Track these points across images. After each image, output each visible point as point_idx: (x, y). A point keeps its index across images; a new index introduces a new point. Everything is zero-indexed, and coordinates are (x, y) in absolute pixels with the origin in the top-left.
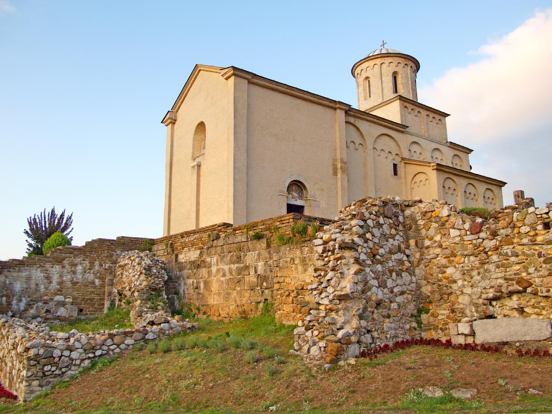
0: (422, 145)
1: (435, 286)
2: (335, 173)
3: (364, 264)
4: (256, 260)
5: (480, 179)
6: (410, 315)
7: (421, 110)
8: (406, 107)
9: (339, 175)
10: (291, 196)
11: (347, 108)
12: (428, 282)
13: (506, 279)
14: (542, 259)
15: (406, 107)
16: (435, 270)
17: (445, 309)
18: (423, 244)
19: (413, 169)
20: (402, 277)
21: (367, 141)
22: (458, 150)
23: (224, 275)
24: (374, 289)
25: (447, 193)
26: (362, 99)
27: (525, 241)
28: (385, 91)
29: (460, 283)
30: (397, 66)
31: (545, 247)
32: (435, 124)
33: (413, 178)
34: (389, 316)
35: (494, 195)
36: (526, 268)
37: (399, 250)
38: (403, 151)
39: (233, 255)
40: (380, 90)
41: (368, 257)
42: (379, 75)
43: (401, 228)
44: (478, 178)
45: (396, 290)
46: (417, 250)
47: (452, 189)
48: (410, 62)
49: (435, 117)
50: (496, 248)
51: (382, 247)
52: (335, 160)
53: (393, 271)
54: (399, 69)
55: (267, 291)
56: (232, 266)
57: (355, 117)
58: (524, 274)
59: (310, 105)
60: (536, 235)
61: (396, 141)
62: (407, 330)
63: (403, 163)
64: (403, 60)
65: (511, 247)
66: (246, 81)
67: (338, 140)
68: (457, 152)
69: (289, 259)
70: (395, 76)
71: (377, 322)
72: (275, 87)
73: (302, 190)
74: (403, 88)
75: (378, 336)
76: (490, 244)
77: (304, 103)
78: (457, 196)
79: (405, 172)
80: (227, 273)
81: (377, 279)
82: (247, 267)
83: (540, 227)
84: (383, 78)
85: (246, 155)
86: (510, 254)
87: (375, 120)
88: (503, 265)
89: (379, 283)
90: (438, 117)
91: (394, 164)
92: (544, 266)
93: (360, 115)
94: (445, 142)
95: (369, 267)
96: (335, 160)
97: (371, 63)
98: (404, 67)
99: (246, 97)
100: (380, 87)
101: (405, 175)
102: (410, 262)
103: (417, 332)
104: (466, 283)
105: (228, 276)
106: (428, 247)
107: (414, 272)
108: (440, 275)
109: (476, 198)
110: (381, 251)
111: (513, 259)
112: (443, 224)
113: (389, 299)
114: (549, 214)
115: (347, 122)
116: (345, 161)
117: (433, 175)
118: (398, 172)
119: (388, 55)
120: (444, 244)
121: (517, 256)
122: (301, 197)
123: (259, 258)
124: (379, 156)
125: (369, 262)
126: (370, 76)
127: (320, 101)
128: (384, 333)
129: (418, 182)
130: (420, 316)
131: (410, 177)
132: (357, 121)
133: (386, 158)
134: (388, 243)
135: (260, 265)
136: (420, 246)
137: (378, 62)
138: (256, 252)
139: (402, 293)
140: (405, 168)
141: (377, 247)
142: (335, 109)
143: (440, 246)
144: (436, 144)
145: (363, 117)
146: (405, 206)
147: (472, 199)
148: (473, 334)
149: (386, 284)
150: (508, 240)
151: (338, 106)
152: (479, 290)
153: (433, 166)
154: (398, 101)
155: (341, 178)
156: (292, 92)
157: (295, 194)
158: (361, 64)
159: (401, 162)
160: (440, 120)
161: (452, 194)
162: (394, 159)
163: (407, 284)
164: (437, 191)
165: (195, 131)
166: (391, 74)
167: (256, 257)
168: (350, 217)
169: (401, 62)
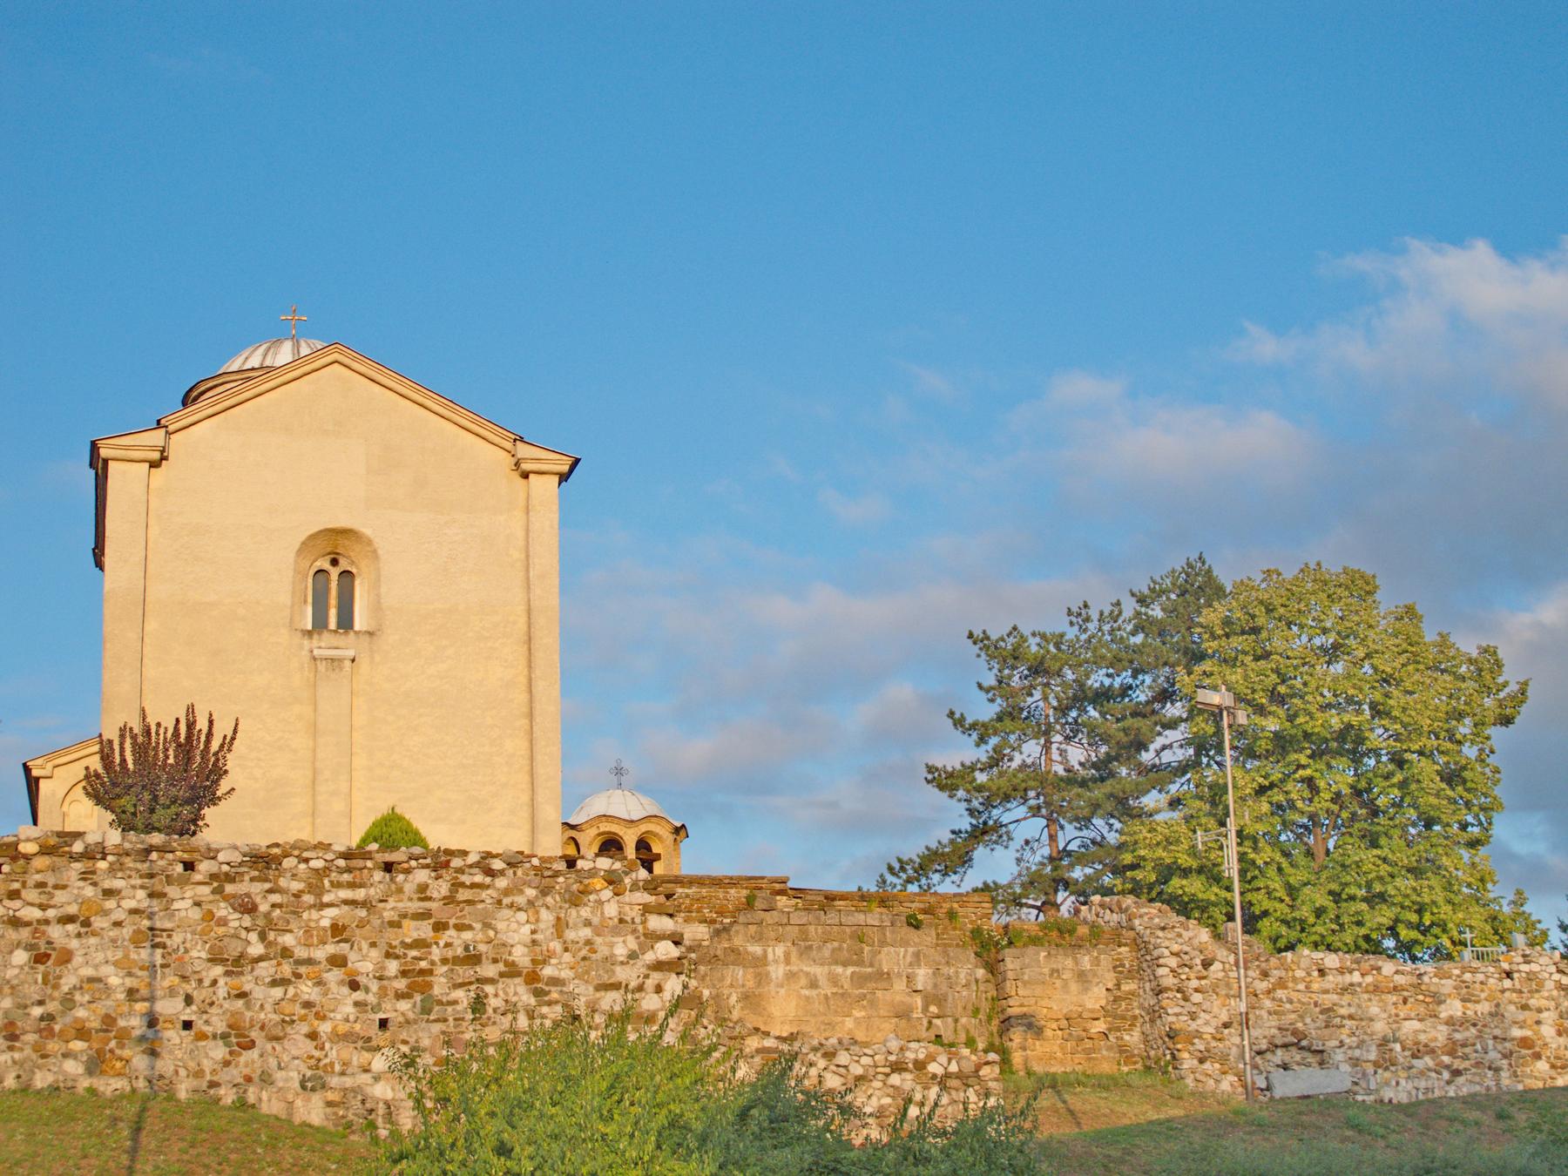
4: (911, 964)
23: (813, 984)
36: (1302, 1017)
39: (840, 949)
50: (1269, 992)
55: (937, 1022)
56: (839, 970)
58: (1300, 1025)
69: (1046, 971)
76: (1262, 986)
80: (823, 981)
82: (884, 977)
83: (1316, 974)
88: (1276, 1013)
105: (828, 990)
111: (1288, 1006)
123: (919, 960)
135: (923, 975)
138: (911, 950)
150: (1281, 984)
165: (303, 543)
167: (909, 959)
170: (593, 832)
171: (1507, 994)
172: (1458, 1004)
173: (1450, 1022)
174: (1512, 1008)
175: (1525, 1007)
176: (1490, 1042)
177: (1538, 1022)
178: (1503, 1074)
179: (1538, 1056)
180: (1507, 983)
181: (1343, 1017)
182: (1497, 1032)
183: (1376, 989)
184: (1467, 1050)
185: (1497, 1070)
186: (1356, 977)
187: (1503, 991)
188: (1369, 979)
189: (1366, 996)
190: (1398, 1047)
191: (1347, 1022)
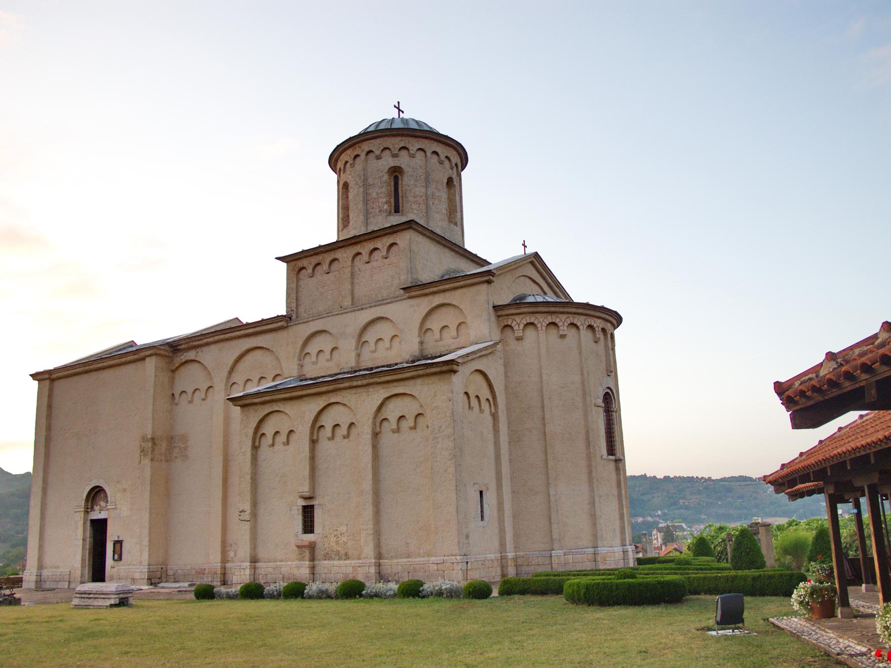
5: (355, 384)
22: (444, 291)
25: (273, 445)
68: (438, 300)
87: (222, 337)
127: (123, 360)
144: (373, 310)
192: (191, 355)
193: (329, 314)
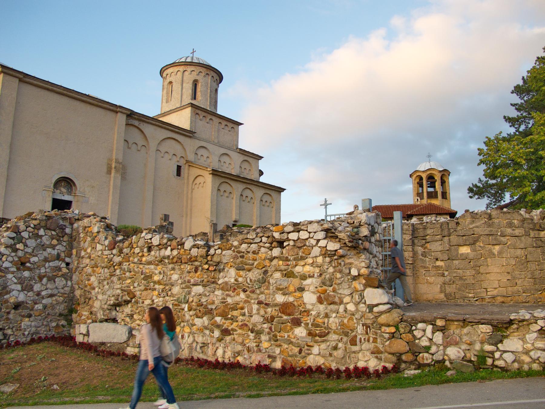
0: (211, 150)
1: (83, 291)
2: (109, 172)
3: (7, 270)
6: (58, 314)
7: (214, 118)
8: (197, 114)
9: (113, 174)
10: (58, 191)
11: (129, 113)
12: (79, 287)
13: (122, 290)
14: (143, 276)
15: (197, 114)
16: (84, 277)
17: (86, 311)
18: (80, 254)
19: (195, 172)
20: (55, 282)
21: (150, 144)
22: (248, 156)
24: (14, 293)
25: (222, 196)
26: (164, 101)
27: (136, 260)
28: (184, 97)
29: (97, 289)
30: (198, 75)
31: (147, 266)
32: (227, 131)
33: (194, 180)
34: (30, 316)
35: (272, 199)
37: (58, 257)
38: (188, 154)
40: (180, 95)
41: (13, 265)
42: (180, 81)
43: (66, 238)
44: (256, 184)
45: (43, 293)
46: (77, 258)
47: (228, 191)
48: (212, 72)
49: (228, 124)
51: (37, 256)
52: (110, 160)
53: (44, 276)
54: (200, 78)
57: (140, 120)
59: (89, 107)
60: (143, 256)
61: (182, 145)
62: (53, 327)
63: (187, 164)
64: (205, 69)
65: (128, 264)
66: (17, 80)
67: (115, 142)
70: (195, 84)
71: (13, 321)
72: (51, 87)
73: (71, 186)
74: (202, 96)
75: (12, 333)
77: (82, 105)
78: (233, 198)
79: (189, 174)
81: (20, 283)
84: (184, 85)
85: (9, 151)
86: (126, 270)
89: (22, 287)
90: (230, 125)
91: (178, 166)
92: (143, 282)
93: (145, 119)
94: (235, 148)
95: (13, 273)
96: (110, 160)
97: (175, 69)
98: (204, 76)
99: (15, 95)
100: (180, 92)
101: (188, 176)
102: (68, 269)
103: (65, 329)
104: (100, 290)
106: (83, 258)
107: (71, 278)
108: (87, 282)
109: (253, 201)
110: (35, 259)
111: (128, 274)
112: (94, 239)
113: (33, 301)
114: (153, 239)
115: (127, 124)
116: (121, 161)
117: (209, 178)
118: (182, 173)
119: (191, 64)
120: (92, 256)
121: (130, 272)
122: (70, 193)
124: (162, 157)
125: (14, 269)
126: (173, 81)
127: (100, 104)
128: (20, 330)
129: (198, 184)
130: (71, 315)
131: (192, 179)
132: (142, 124)
133: (170, 159)
134: (44, 252)
136: (78, 256)
137: (181, 69)
139: (51, 296)
140: (189, 170)
141: (28, 256)
142: (117, 112)
143: (90, 257)
145: (148, 121)
146: (76, 220)
147: (249, 202)
148: (88, 334)
149: (33, 287)
151: (118, 109)
152: (106, 297)
153: (209, 171)
154: (190, 109)
155: (114, 177)
156: (69, 93)
157: (63, 190)
158: (167, 69)
159: (185, 164)
160: (232, 127)
161: (227, 197)
162: (178, 161)
163: (60, 287)
164: (210, 194)
166: (192, 82)
168: (5, 229)
169: (203, 72)
170: (415, 176)
171: (275, 262)
172: (232, 272)
173: (225, 287)
174: (278, 275)
175: (289, 275)
176: (255, 307)
177: (301, 289)
178: (264, 337)
179: (297, 323)
180: (276, 252)
181: (155, 283)
182: (262, 297)
183: (179, 261)
184: (235, 313)
185: (258, 333)
186: (168, 252)
187: (272, 259)
188: (175, 252)
189: (171, 266)
190: (186, 307)
191: (157, 286)
192: (136, 123)
193: (209, 142)
